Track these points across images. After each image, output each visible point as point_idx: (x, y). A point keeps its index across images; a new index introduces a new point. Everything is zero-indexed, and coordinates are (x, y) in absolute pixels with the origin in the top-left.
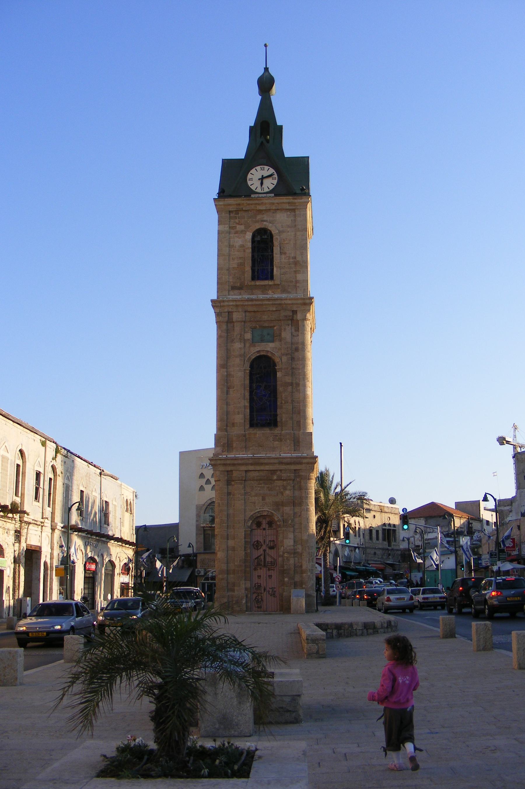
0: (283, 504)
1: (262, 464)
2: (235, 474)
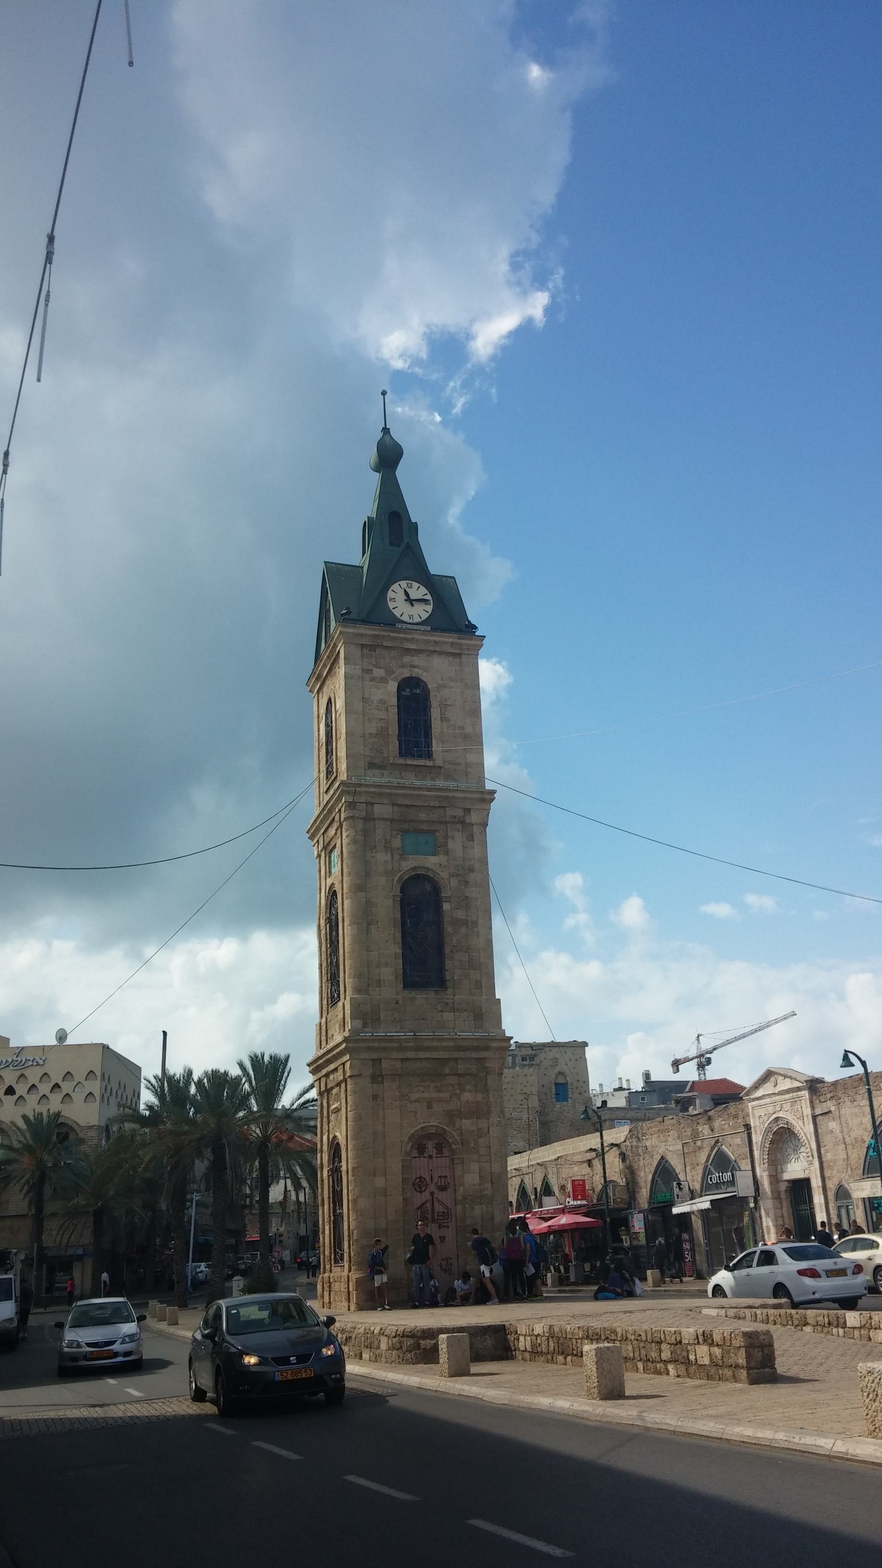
2: (385, 1064)
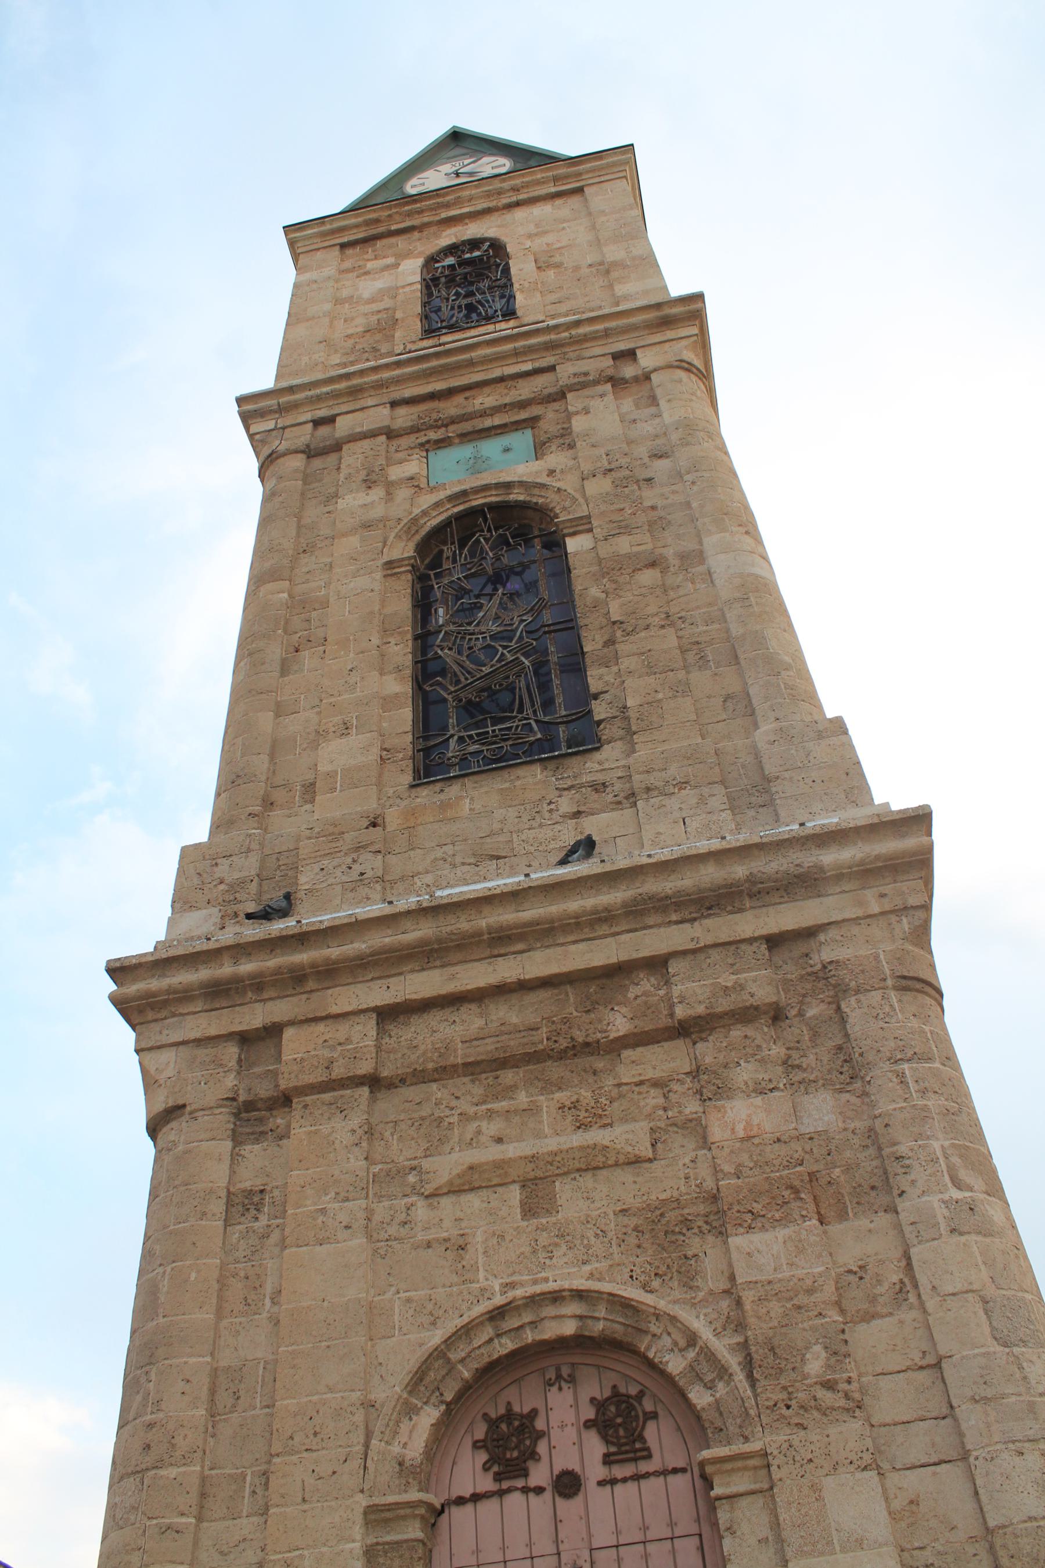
0: (718, 1215)
1: (501, 941)
